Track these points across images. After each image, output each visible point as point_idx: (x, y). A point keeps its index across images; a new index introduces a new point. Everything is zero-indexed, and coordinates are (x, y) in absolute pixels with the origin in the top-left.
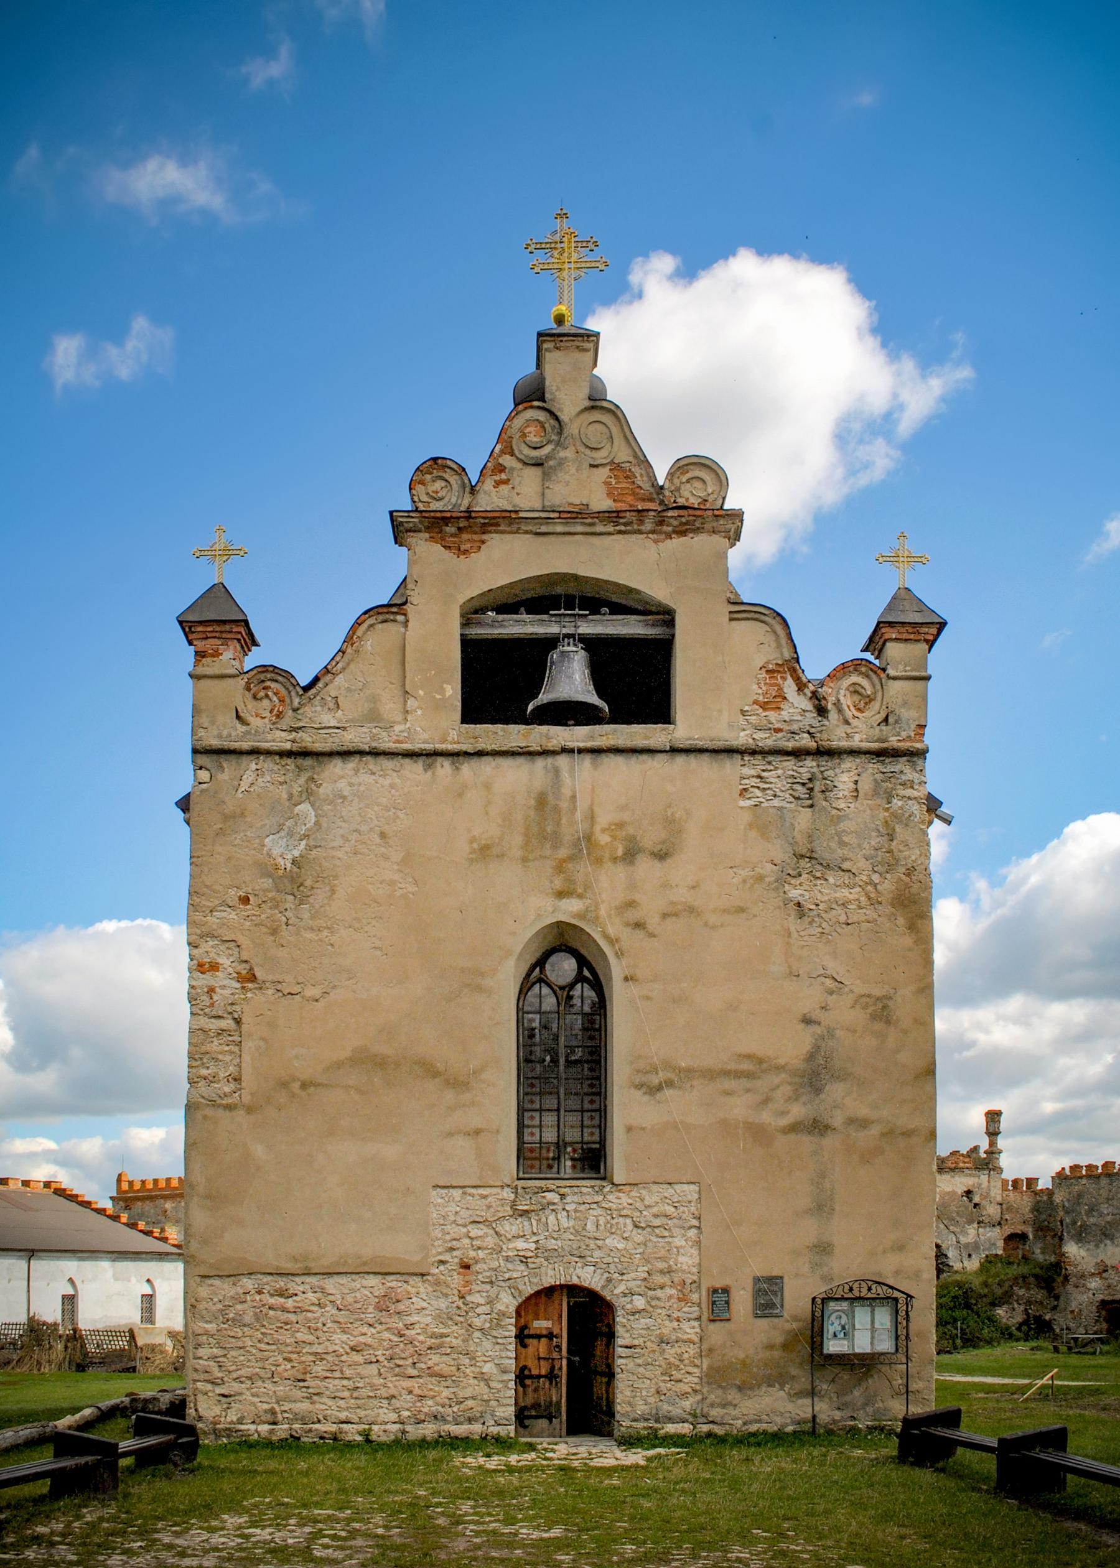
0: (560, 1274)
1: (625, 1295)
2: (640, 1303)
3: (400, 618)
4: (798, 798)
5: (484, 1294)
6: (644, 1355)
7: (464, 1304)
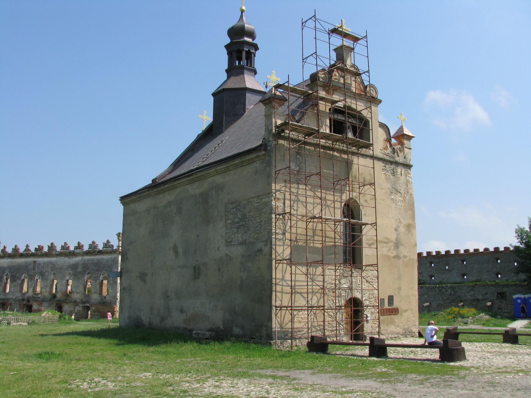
3: (316, 109)
4: (392, 173)
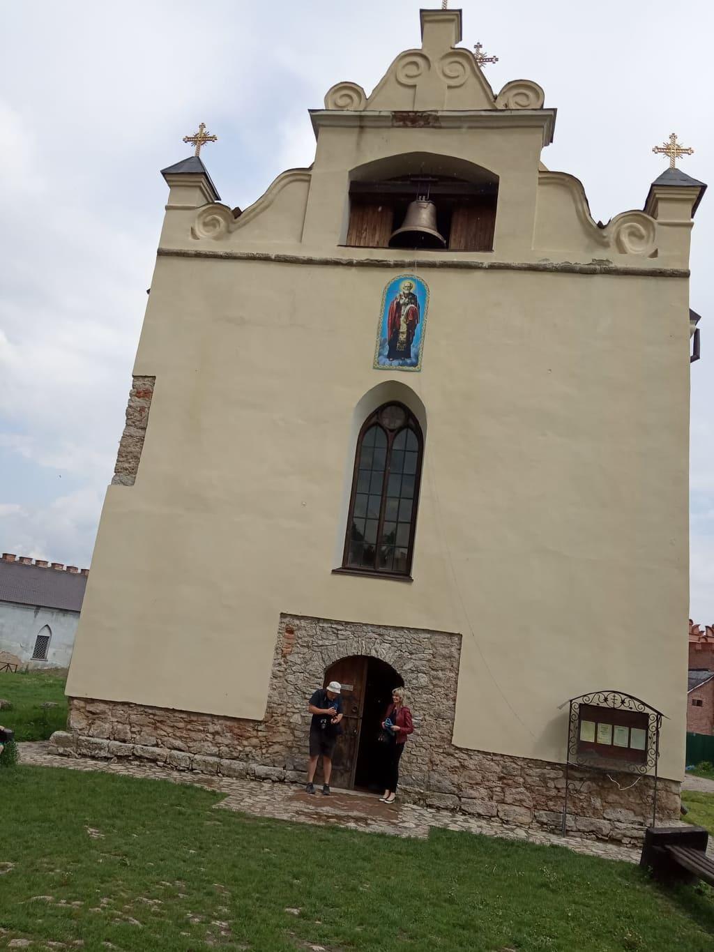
0: (362, 647)
1: (413, 672)
2: (424, 680)
5: (301, 656)
6: (422, 726)
7: (284, 662)
